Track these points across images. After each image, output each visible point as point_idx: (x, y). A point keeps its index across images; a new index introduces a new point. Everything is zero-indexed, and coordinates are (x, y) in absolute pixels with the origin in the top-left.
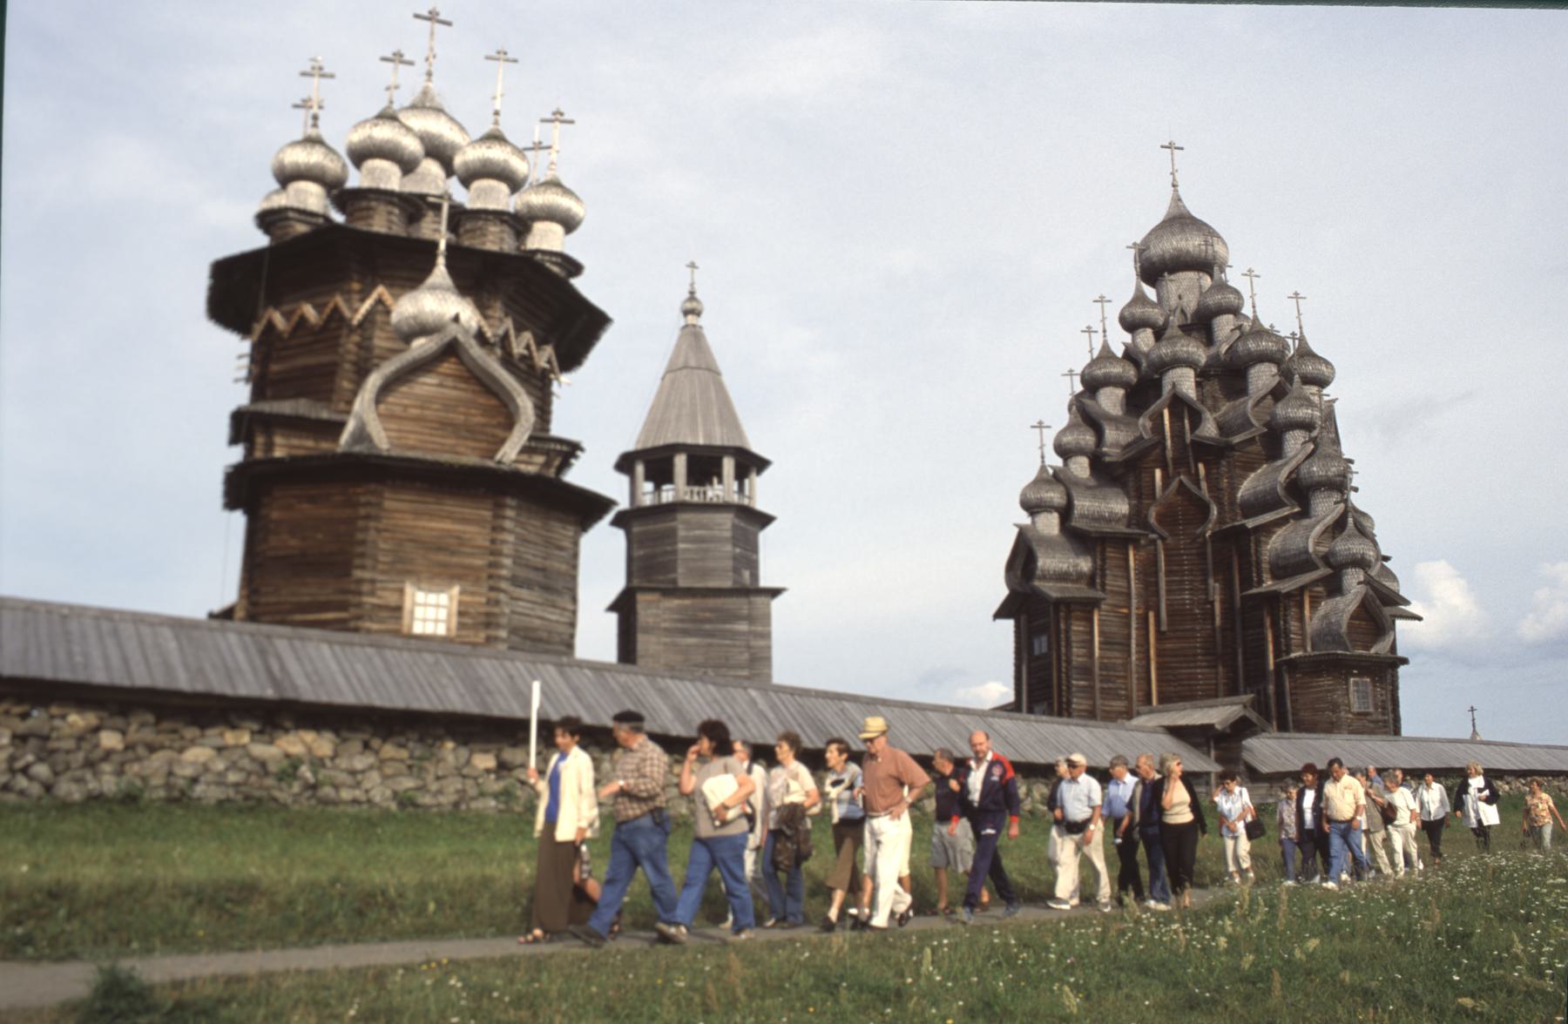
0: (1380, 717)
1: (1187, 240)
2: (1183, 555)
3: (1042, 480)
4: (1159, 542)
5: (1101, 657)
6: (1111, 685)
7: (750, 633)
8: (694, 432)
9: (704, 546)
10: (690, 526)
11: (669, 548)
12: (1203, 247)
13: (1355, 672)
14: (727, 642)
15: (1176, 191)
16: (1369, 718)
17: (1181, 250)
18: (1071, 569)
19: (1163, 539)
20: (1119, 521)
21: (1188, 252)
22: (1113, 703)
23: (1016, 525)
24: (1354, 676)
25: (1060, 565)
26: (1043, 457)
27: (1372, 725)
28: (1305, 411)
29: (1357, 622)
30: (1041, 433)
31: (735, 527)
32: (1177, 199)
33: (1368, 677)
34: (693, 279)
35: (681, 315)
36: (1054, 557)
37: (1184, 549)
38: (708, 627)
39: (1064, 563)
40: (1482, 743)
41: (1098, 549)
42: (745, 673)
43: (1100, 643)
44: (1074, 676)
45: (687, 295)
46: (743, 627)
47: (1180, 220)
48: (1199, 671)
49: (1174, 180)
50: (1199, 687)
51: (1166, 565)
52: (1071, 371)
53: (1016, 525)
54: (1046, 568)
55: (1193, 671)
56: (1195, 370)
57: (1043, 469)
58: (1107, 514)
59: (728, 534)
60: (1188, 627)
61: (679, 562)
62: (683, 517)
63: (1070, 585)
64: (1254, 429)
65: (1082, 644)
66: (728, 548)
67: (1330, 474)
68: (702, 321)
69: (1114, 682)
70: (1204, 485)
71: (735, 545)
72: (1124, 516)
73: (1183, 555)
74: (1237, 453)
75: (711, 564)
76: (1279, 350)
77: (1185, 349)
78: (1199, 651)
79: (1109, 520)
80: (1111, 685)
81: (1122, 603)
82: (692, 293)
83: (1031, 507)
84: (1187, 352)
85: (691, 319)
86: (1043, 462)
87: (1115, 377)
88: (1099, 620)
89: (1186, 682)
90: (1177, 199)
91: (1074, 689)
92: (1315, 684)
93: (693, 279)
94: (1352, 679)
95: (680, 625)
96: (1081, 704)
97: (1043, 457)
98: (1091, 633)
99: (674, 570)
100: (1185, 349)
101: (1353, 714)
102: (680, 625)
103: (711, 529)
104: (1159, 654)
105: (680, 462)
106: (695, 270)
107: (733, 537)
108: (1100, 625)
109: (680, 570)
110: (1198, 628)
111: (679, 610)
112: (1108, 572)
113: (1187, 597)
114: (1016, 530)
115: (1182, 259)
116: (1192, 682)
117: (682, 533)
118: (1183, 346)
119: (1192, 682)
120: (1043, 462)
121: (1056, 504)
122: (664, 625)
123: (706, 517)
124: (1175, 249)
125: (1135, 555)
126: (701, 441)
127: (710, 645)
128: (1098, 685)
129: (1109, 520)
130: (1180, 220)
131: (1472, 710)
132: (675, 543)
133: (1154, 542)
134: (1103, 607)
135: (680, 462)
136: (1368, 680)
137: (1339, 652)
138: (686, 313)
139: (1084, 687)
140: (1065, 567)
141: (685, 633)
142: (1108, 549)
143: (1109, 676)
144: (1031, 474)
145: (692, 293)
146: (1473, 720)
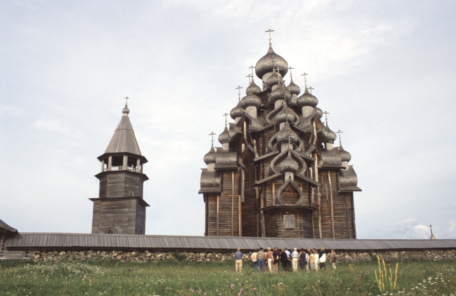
0: (299, 230)
1: (266, 62)
2: (249, 174)
3: (212, 152)
4: (242, 170)
5: (219, 213)
6: (224, 223)
7: (129, 211)
8: (115, 149)
9: (115, 184)
10: (111, 179)
11: (105, 186)
12: (272, 63)
13: (287, 213)
14: (121, 215)
15: (271, 46)
16: (293, 231)
17: (264, 65)
18: (213, 182)
19: (244, 169)
20: (233, 164)
21: (266, 66)
22: (225, 230)
23: (201, 169)
24: (286, 214)
25: (209, 181)
26: (212, 145)
27: (295, 234)
28: (283, 115)
29: (289, 193)
30: (212, 136)
31: (125, 177)
32: (271, 48)
33: (293, 214)
34: (127, 102)
35: (123, 113)
36: (207, 179)
37: (250, 171)
38: (115, 210)
39: (210, 180)
40: (436, 240)
41: (221, 175)
42: (127, 224)
43: (219, 208)
44: (209, 220)
45: (125, 107)
46: (127, 210)
47: (271, 54)
48: (253, 216)
49: (270, 42)
50: (253, 222)
51: (245, 178)
52: (226, 114)
53: (201, 169)
54: (204, 182)
55: (251, 216)
56: (257, 107)
57: (212, 149)
58: (228, 162)
59: (124, 180)
60: (250, 200)
61: (107, 190)
62: (109, 176)
63: (214, 188)
64: (268, 125)
65: (213, 209)
66: (123, 185)
67: (283, 137)
68: (129, 115)
69: (226, 222)
70: (255, 147)
71: (125, 184)
72: (235, 162)
73: (249, 174)
74: (266, 134)
75: (118, 190)
76: (282, 94)
77: (248, 99)
78: (253, 209)
79: (230, 164)
80: (224, 223)
81: (230, 193)
82: (126, 106)
83: (207, 162)
84: (249, 100)
85: (125, 115)
86: (212, 146)
87: (238, 114)
88: (219, 200)
89: (249, 221)
90: (271, 48)
91: (209, 225)
92: (271, 218)
93: (127, 102)
94: (285, 216)
95: (106, 210)
96: (212, 230)
97: (212, 145)
98: (216, 204)
99: (106, 193)
100: (248, 99)
101: (285, 229)
102: (106, 210)
103: (118, 179)
104: (242, 211)
105: (125, 159)
106: (128, 99)
107: (125, 181)
108: (219, 201)
109: (107, 193)
110: (253, 200)
111: (108, 205)
112: (224, 182)
113: (250, 189)
114: (201, 171)
115: (265, 68)
116: (251, 220)
117: (109, 181)
118: (247, 98)
119: (251, 220)
120: (212, 146)
121: (212, 160)
122: (102, 210)
123: (116, 175)
124: (262, 66)
125: (234, 175)
126: (117, 152)
127: (116, 216)
128: (218, 223)
129: (230, 164)
130: (271, 54)
131: (431, 226)
132: (107, 184)
133: (241, 170)
134: (222, 195)
135: (125, 159)
136: (293, 216)
137: (287, 205)
138: (124, 112)
139: (214, 224)
140: (210, 182)
141: (108, 213)
142: (224, 174)
143: (224, 220)
144: (208, 150)
145: (126, 106)
146: (431, 230)
